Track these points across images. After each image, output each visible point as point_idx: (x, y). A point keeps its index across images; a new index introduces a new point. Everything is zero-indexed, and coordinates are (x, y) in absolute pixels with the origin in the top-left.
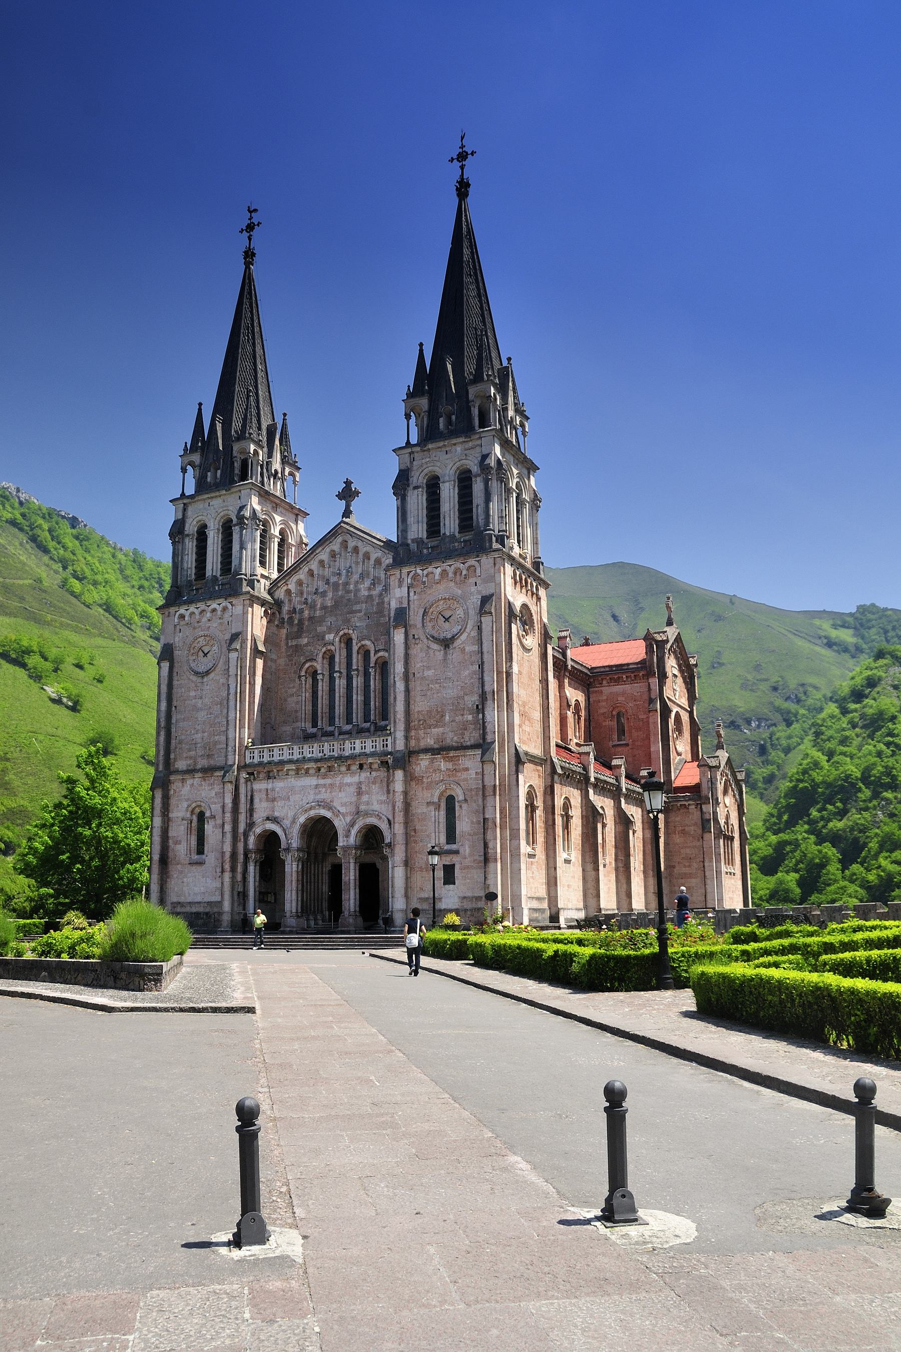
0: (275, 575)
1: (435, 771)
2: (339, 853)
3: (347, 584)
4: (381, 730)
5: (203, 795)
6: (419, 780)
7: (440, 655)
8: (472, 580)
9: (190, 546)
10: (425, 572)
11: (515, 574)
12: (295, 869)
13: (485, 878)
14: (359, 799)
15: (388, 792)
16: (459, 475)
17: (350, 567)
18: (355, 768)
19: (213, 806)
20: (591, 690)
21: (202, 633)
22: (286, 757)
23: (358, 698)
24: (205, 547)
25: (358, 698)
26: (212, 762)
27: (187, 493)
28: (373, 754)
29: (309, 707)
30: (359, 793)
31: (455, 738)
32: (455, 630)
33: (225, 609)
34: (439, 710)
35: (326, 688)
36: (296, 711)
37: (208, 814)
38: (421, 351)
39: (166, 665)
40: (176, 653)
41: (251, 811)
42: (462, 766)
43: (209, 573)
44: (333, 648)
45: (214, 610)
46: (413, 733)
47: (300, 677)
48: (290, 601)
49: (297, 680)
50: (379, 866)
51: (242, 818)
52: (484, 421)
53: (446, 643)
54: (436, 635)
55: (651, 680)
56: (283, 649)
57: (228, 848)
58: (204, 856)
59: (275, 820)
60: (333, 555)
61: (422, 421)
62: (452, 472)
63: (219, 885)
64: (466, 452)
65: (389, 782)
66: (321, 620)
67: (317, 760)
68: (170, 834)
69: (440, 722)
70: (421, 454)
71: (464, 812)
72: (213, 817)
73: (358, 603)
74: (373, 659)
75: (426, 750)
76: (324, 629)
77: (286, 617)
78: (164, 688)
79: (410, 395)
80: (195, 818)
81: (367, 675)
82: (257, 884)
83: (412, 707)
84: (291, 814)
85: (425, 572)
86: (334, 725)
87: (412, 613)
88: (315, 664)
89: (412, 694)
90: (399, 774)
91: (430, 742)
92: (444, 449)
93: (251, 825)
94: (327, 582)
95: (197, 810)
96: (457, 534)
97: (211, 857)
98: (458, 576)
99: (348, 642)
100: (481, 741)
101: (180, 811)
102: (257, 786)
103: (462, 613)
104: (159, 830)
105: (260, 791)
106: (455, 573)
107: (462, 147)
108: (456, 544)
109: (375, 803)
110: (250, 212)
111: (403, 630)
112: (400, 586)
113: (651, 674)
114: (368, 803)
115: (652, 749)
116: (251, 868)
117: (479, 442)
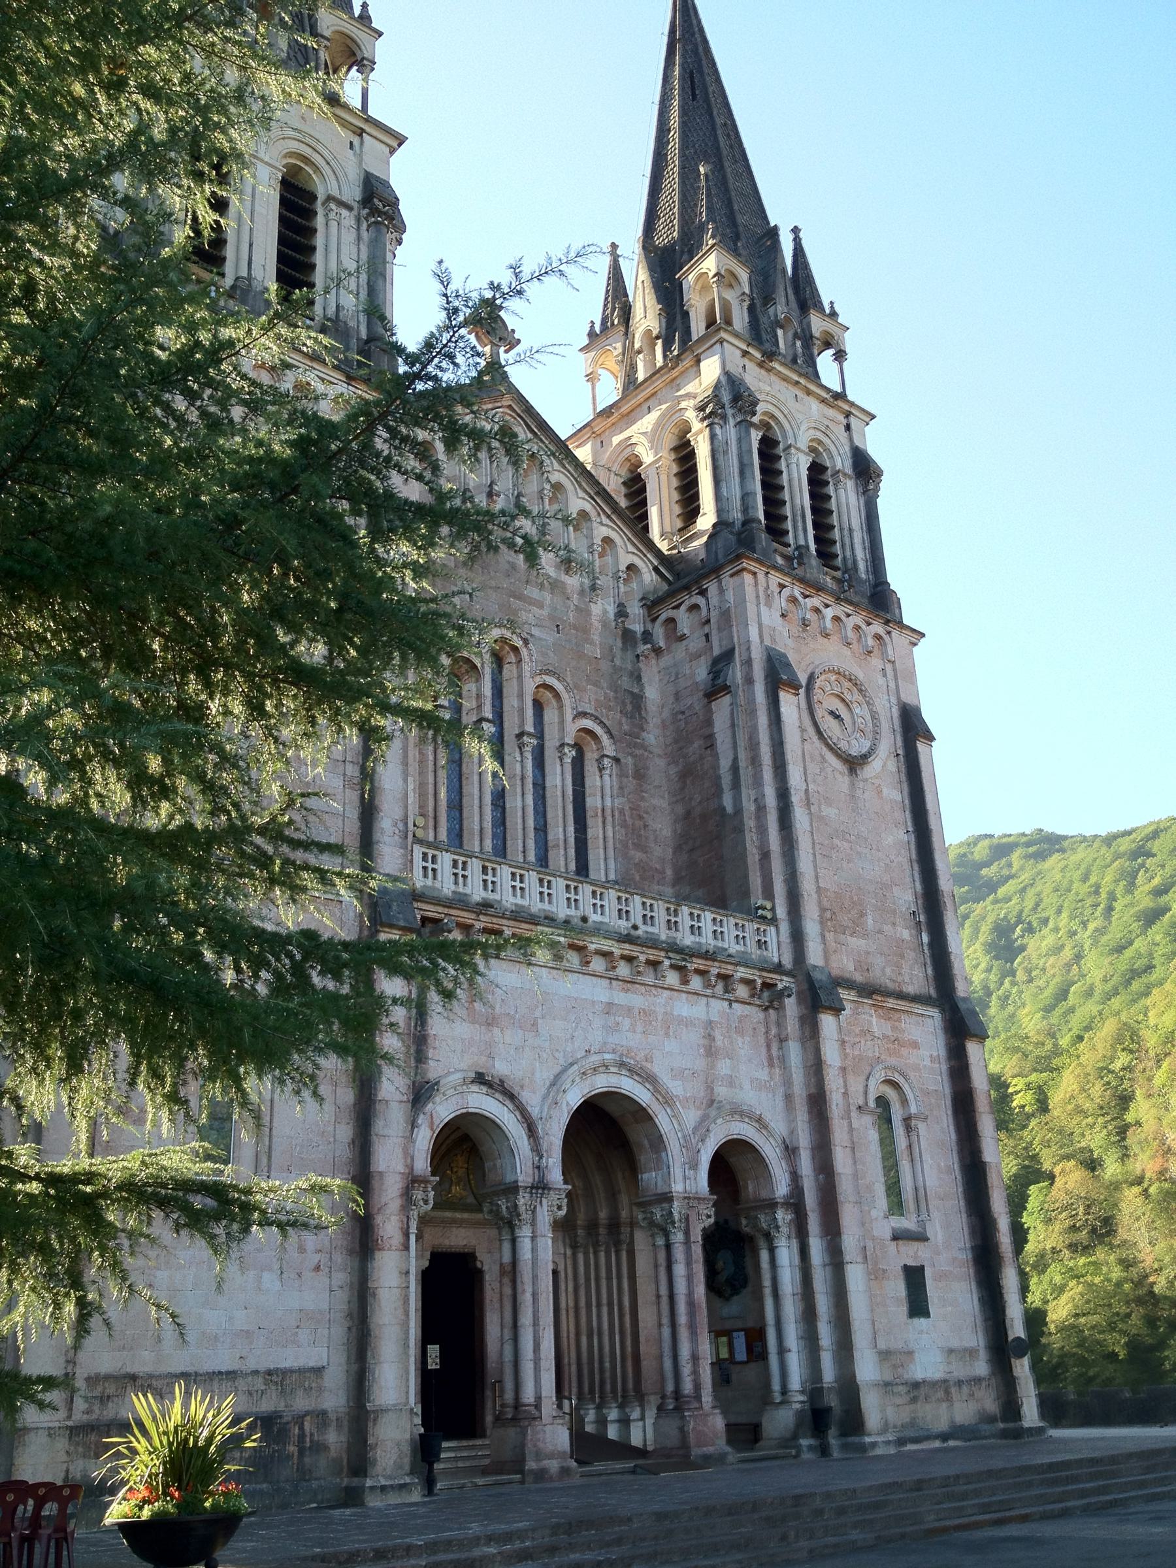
8: (876, 662)
14: (712, 1066)
30: (711, 1052)
34: (855, 898)
53: (854, 764)
84: (544, 1075)
103: (868, 717)
109: (747, 1086)
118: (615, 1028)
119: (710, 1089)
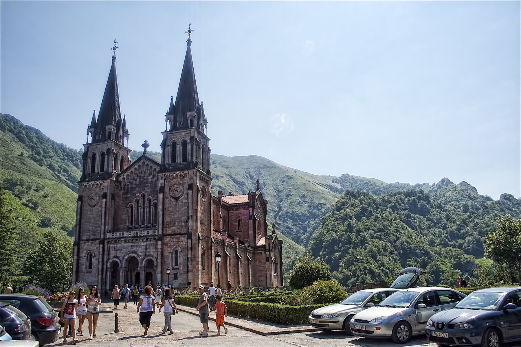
0: (119, 172)
1: (172, 242)
2: (139, 269)
3: (144, 176)
4: (154, 227)
5: (92, 248)
6: (166, 245)
7: (174, 203)
8: (186, 178)
9: (89, 161)
10: (170, 175)
11: (200, 176)
12: (123, 274)
13: (187, 277)
14: (146, 250)
15: (156, 248)
16: (183, 142)
17: (145, 171)
18: (145, 240)
19: (95, 252)
20: (229, 212)
21: (93, 192)
22: (121, 236)
23: (146, 216)
24: (95, 162)
25: (146, 216)
26: (95, 237)
27: (89, 142)
28: (151, 236)
29: (130, 218)
30: (146, 249)
31: (179, 231)
32: (180, 195)
33: (101, 184)
35: (136, 212)
36: (125, 220)
37: (93, 255)
38: (172, 99)
39: (80, 203)
40: (84, 199)
41: (109, 254)
42: (181, 240)
43: (96, 171)
44: (139, 198)
45: (97, 184)
46: (165, 229)
47: (127, 208)
48: (124, 181)
49: (126, 209)
50: (153, 273)
51: (105, 256)
52: (192, 125)
53: (177, 199)
54: (173, 196)
55: (250, 209)
56: (122, 198)
57: (100, 267)
58: (91, 270)
59: (117, 257)
60: (140, 166)
61: (171, 123)
62: (181, 141)
63: (97, 279)
64: (186, 135)
65: (156, 245)
66: (135, 189)
67: (132, 237)
68: (80, 262)
69: (174, 225)
70: (171, 134)
71: (181, 256)
72: (95, 256)
73: (148, 183)
74: (152, 203)
75: (169, 235)
76: (136, 192)
77: (123, 187)
78: (79, 211)
79: (168, 114)
80: (89, 256)
81: (150, 208)
82: (110, 279)
83: (165, 220)
84: (123, 255)
85: (170, 175)
86: (138, 225)
87: (165, 189)
88: (132, 204)
89: (165, 216)
90: (160, 243)
91: (170, 232)
92: (178, 133)
93: (108, 259)
94: (137, 176)
95: (90, 253)
96: (181, 162)
97: (94, 270)
98: (181, 177)
99: (144, 196)
100: (187, 232)
101: (83, 254)
102: (111, 245)
104: (76, 260)
105: (112, 247)
106: (180, 176)
107: (190, 28)
108: (181, 166)
110: (115, 43)
111: (162, 194)
112: (162, 179)
113: (249, 207)
114: (149, 252)
115: (250, 233)
116: (108, 274)
117: (190, 132)
118: (133, 248)
119: (145, 253)
